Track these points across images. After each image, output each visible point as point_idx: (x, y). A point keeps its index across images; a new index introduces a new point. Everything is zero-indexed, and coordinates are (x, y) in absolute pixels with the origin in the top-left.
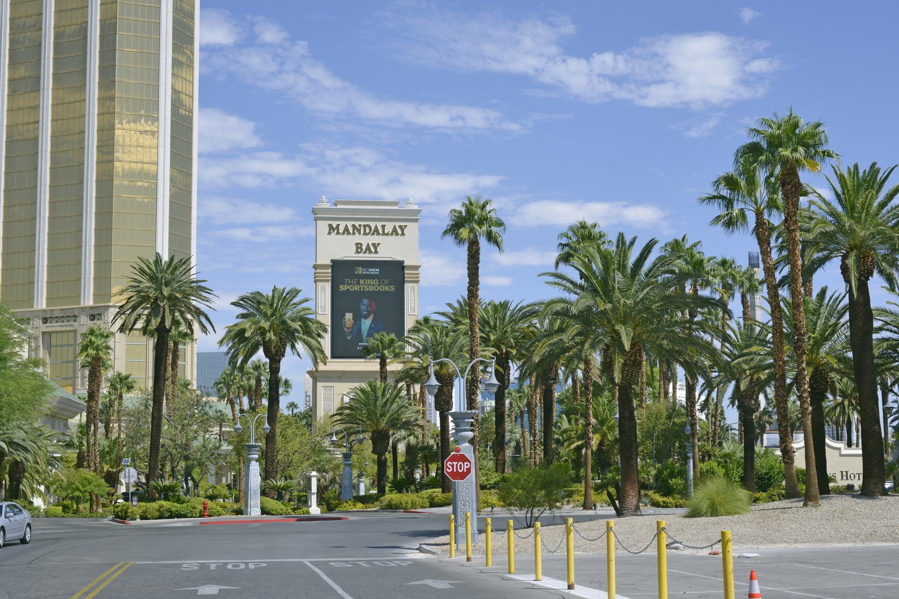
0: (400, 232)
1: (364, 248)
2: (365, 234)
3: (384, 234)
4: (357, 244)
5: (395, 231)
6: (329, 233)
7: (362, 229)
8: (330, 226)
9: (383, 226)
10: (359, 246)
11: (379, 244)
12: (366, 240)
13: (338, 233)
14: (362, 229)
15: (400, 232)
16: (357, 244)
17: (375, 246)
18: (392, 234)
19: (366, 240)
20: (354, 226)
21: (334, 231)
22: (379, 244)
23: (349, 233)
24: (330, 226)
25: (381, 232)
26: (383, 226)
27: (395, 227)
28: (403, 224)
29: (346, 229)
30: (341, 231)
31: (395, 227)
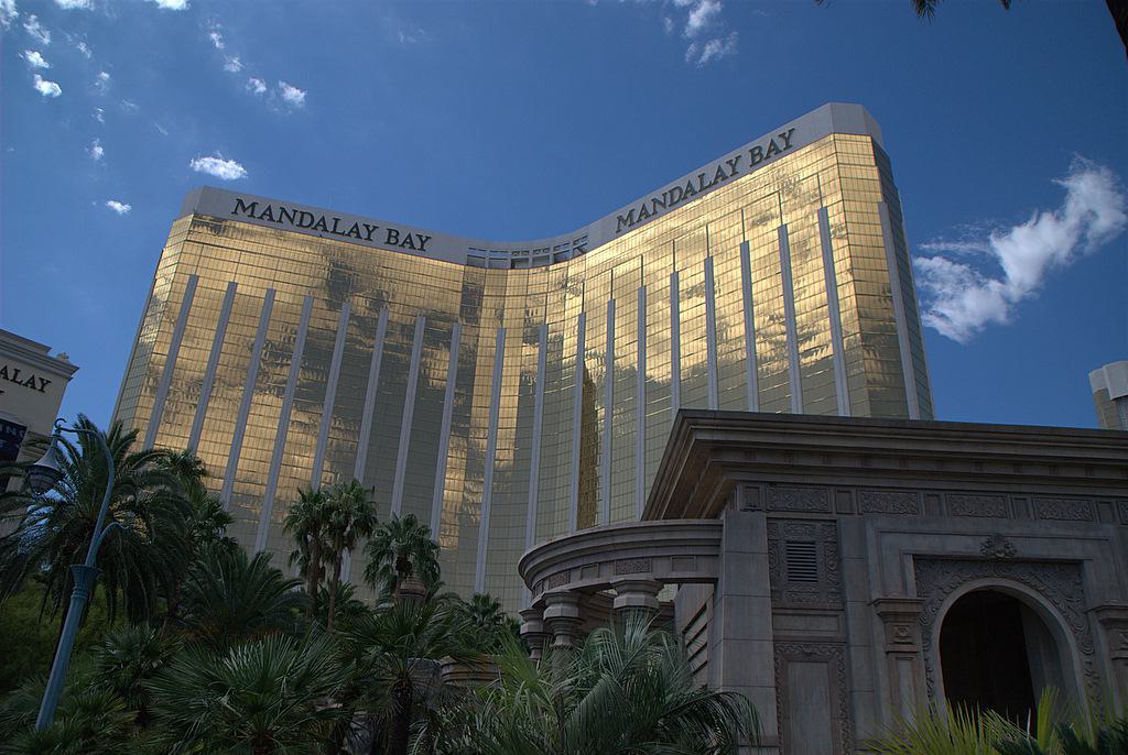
0: (38, 385)
3: (14, 380)
5: (31, 382)
9: (17, 371)
15: (38, 385)
18: (26, 385)
25: (11, 377)
26: (17, 371)
28: (46, 377)
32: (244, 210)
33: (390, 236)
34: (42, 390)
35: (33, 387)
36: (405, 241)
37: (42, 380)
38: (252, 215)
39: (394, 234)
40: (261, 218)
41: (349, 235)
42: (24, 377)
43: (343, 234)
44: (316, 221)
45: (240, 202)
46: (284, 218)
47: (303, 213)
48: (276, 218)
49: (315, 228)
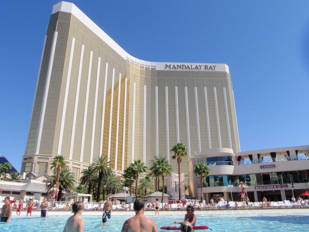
32: (168, 67)
33: (206, 67)
36: (210, 68)
38: (170, 68)
39: (207, 66)
40: (173, 68)
41: (195, 69)
43: (194, 69)
44: (186, 66)
45: (167, 65)
46: (179, 67)
47: (183, 65)
48: (176, 68)
49: (187, 69)
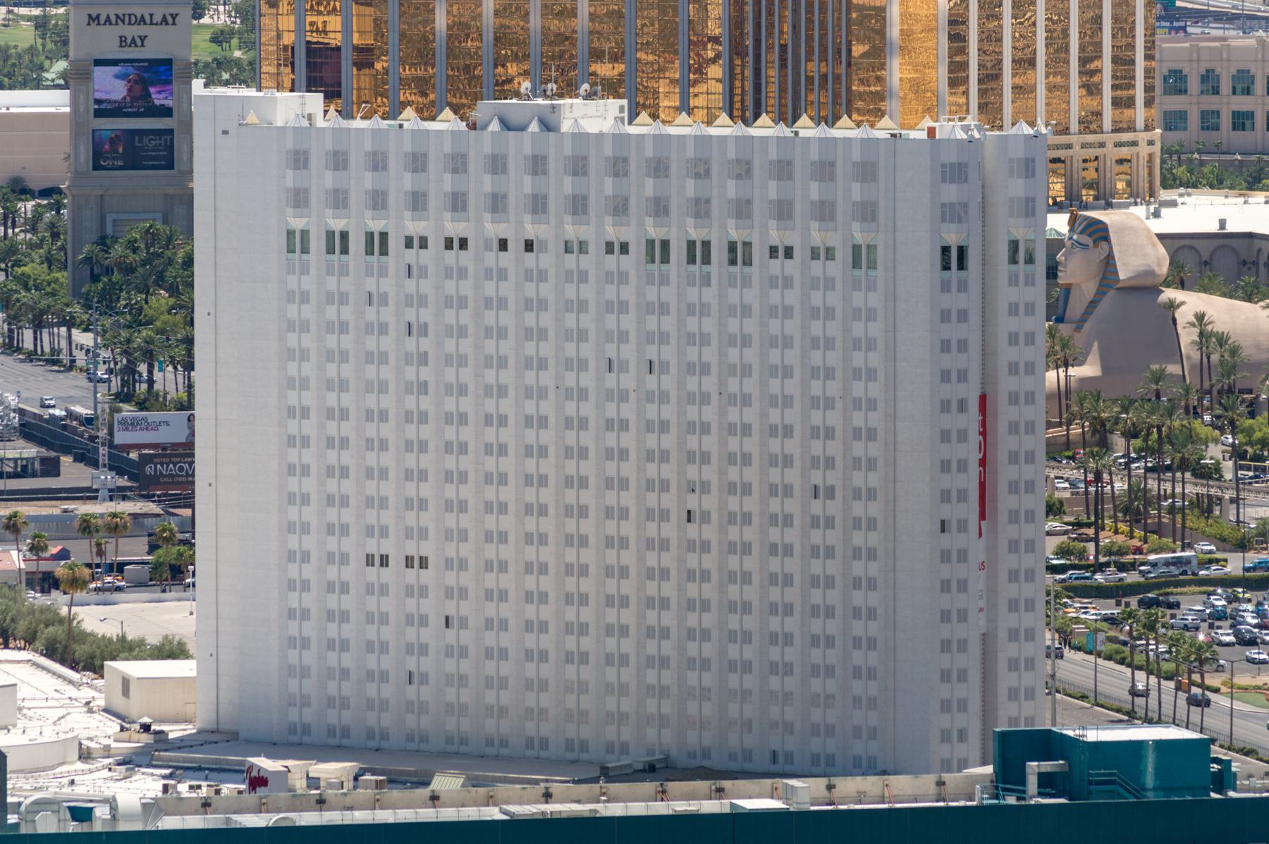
0: (170, 20)
1: (129, 41)
2: (130, 24)
3: (151, 23)
4: (121, 37)
5: (164, 20)
6: (89, 24)
7: (127, 17)
8: (90, 16)
9: (151, 15)
10: (123, 41)
11: (146, 37)
12: (132, 31)
13: (99, 24)
14: (127, 17)
15: (170, 20)
16: (121, 37)
17: (143, 39)
19: (132, 31)
20: (117, 16)
21: (94, 21)
22: (146, 37)
23: (111, 24)
24: (90, 16)
25: (148, 20)
26: (151, 15)
27: (164, 16)
28: (174, 11)
29: (108, 20)
30: (102, 21)
31: (164, 16)
34: (174, 24)
35: (167, 24)
37: (171, 15)
42: (158, 18)
